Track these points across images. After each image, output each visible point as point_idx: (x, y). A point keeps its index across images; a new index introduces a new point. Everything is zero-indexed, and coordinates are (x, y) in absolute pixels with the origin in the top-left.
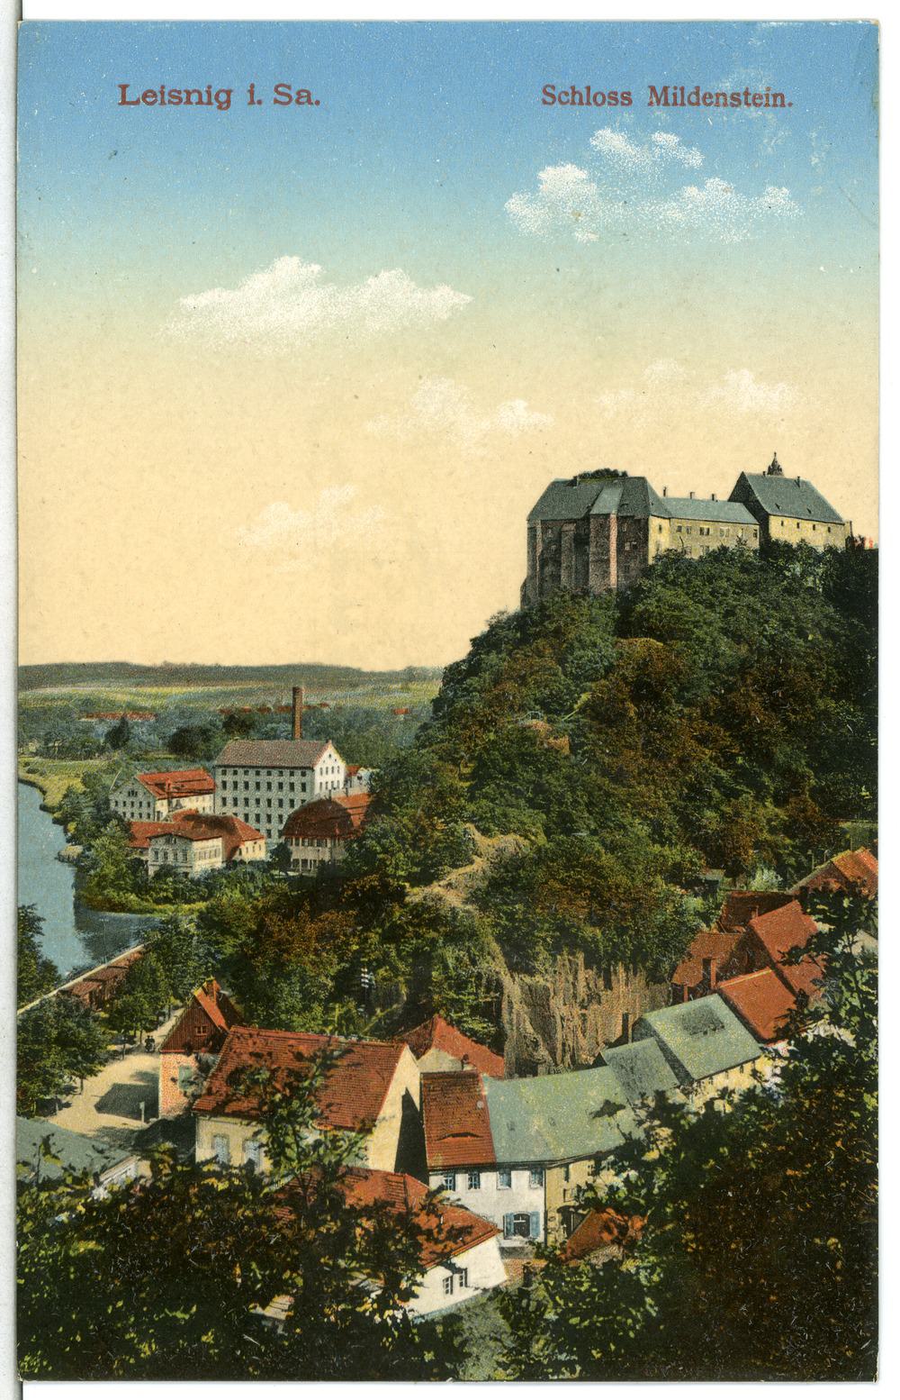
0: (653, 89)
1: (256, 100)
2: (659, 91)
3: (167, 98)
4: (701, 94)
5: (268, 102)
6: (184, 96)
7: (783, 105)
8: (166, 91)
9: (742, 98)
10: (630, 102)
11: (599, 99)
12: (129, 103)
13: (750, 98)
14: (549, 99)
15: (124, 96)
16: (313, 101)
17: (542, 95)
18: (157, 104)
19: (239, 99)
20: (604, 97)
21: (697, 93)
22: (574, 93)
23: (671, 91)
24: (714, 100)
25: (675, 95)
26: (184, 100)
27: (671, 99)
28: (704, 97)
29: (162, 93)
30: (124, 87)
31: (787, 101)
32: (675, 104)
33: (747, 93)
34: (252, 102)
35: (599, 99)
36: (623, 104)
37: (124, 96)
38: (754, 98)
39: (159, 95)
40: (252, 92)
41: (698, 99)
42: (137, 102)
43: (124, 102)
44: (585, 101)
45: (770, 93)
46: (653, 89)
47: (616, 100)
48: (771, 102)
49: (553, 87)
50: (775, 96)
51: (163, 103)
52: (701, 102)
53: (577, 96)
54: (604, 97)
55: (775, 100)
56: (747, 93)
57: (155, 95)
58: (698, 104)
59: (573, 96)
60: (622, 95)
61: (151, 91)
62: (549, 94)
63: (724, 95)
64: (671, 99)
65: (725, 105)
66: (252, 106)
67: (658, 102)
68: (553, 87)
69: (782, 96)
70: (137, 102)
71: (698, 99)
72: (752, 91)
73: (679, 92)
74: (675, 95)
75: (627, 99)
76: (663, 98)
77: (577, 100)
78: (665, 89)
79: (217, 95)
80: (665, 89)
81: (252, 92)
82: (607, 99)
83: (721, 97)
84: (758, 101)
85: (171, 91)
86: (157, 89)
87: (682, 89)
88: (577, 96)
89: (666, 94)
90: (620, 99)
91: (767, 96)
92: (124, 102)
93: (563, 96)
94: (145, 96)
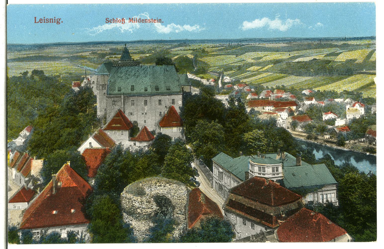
0: (130, 19)
2: (131, 19)
3: (46, 21)
4: (141, 20)
13: (153, 22)
15: (35, 20)
21: (140, 20)
24: (144, 21)
26: (49, 22)
29: (44, 19)
30: (35, 18)
31: (162, 21)
37: (35, 20)
39: (43, 20)
42: (38, 22)
43: (35, 22)
45: (158, 19)
48: (158, 21)
50: (159, 20)
51: (44, 22)
57: (42, 20)
58: (140, 22)
60: (48, 21)
61: (41, 19)
66: (45, 23)
67: (131, 22)
69: (161, 20)
70: (38, 22)
74: (135, 20)
78: (132, 18)
84: (155, 21)
86: (43, 19)
87: (136, 19)
94: (40, 20)
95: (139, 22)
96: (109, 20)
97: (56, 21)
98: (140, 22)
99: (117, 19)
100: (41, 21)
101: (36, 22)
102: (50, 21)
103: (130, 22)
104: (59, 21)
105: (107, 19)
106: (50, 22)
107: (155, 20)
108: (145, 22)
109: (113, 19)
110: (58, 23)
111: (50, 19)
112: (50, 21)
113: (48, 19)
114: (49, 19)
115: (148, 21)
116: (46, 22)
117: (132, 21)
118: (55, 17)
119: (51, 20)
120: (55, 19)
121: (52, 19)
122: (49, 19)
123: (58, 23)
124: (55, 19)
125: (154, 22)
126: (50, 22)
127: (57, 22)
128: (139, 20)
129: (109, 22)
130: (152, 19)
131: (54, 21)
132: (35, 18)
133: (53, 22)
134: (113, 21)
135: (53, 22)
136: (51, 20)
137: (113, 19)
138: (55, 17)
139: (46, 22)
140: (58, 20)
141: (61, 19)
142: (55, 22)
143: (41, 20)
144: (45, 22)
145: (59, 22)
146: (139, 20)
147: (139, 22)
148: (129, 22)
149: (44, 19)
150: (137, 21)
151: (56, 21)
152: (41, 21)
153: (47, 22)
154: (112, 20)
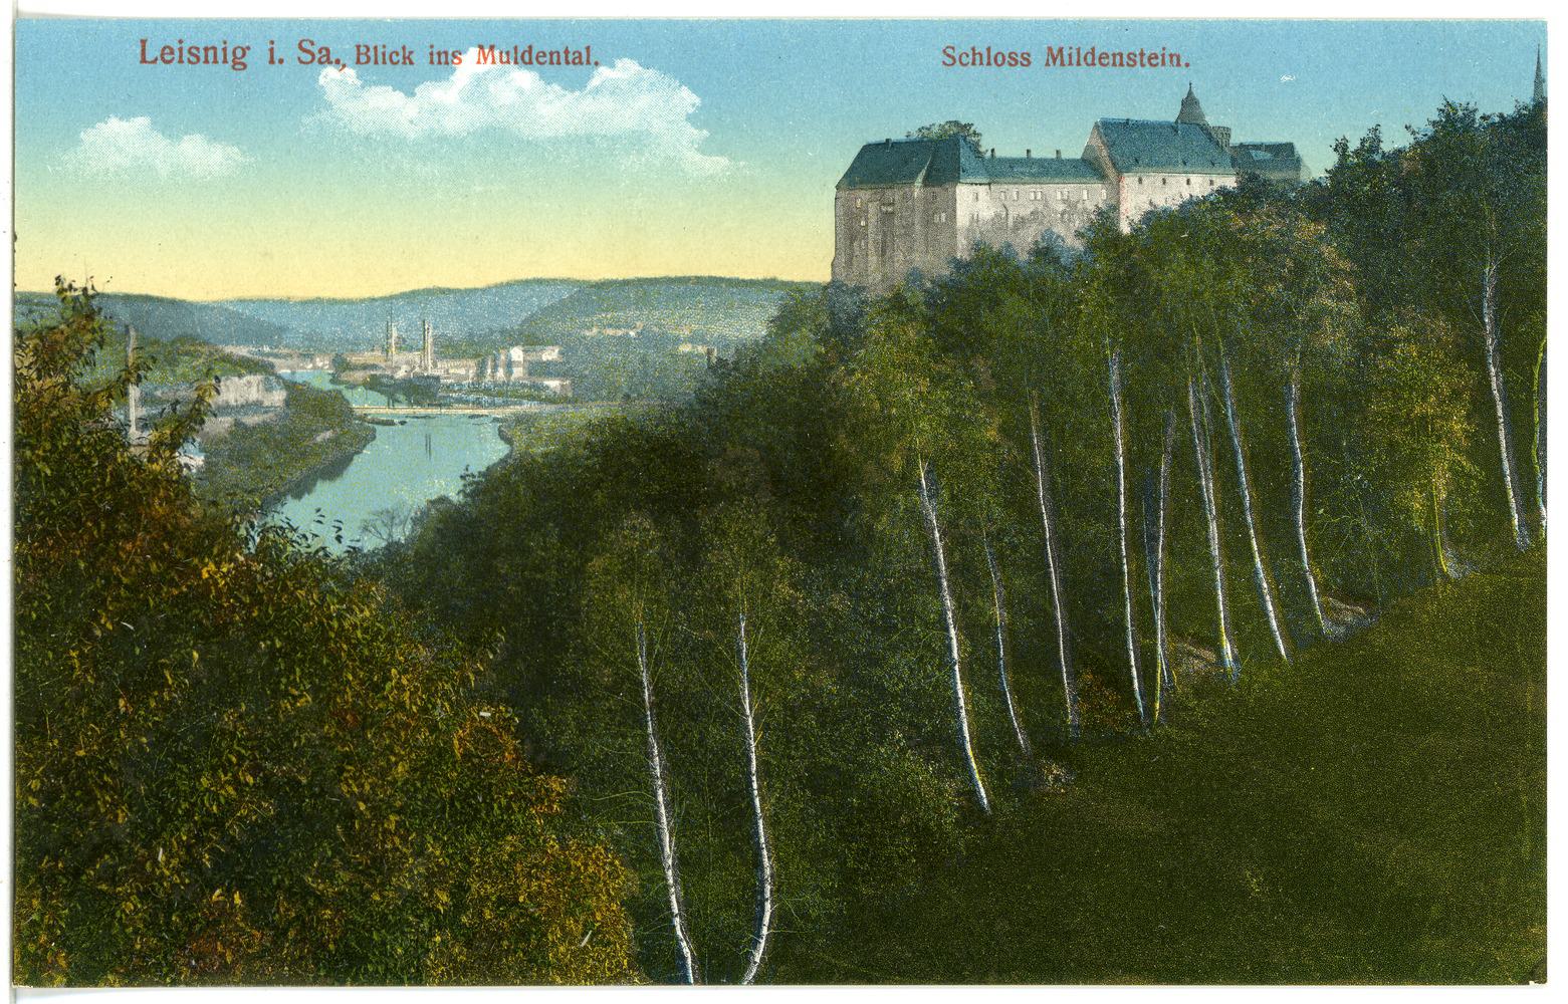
0: (1050, 49)
1: (277, 57)
2: (1055, 52)
4: (1097, 55)
5: (291, 62)
6: (202, 54)
7: (1178, 65)
8: (186, 46)
9: (1138, 59)
10: (1029, 63)
11: (1000, 58)
12: (149, 63)
13: (1145, 61)
14: (949, 61)
16: (333, 59)
18: (175, 62)
20: (1004, 59)
22: (974, 54)
23: (1066, 53)
25: (1070, 55)
26: (202, 59)
27: (1066, 61)
28: (1100, 58)
29: (181, 49)
30: (143, 42)
31: (1182, 63)
32: (1070, 64)
33: (1142, 54)
34: (272, 62)
35: (1000, 61)
36: (1022, 65)
38: (1150, 59)
39: (177, 54)
40: (272, 50)
41: (1093, 59)
42: (156, 59)
43: (144, 61)
46: (1050, 49)
47: (1016, 62)
51: (181, 61)
52: (1096, 61)
54: (1004, 59)
56: (1142, 54)
57: (172, 53)
58: (1094, 64)
61: (168, 47)
62: (949, 56)
64: (1066, 61)
65: (1121, 64)
67: (1054, 63)
71: (1093, 59)
74: (1070, 55)
76: (1058, 62)
77: (978, 62)
78: (1061, 50)
79: (234, 53)
80: (1061, 50)
81: (272, 50)
82: (1008, 59)
83: (1118, 58)
84: (1154, 62)
85: (190, 49)
86: (176, 46)
87: (1078, 50)
89: (1062, 57)
90: (1019, 59)
91: (1163, 55)
92: (144, 61)
94: (162, 55)
95: (1089, 60)
97: (230, 57)
99: (989, 49)
100: (166, 55)
101: (149, 58)
102: (206, 56)
104: (244, 55)
105: (950, 51)
106: (206, 62)
107: (1157, 57)
108: (1114, 64)
109: (973, 49)
110: (239, 64)
111: (206, 49)
112: (206, 56)
113: (198, 49)
114: (201, 46)
115: (1125, 59)
116: (189, 61)
117: (1058, 62)
118: (225, 43)
119: (211, 53)
120: (225, 50)
121: (214, 48)
122: (201, 46)
123: (237, 67)
124: (225, 50)
125: (1151, 65)
126: (206, 62)
127: (233, 61)
128: (1089, 58)
129: (958, 63)
132: (143, 42)
133: (215, 62)
135: (215, 62)
136: (211, 53)
137: (973, 49)
139: (189, 61)
140: (239, 53)
141: (248, 48)
142: (225, 61)
143: (167, 51)
144: (185, 59)
145: (243, 60)
146: (1089, 58)
147: (1089, 60)
148: (1047, 64)
149: (181, 49)
150: (1082, 59)
151: (230, 57)
153: (194, 59)
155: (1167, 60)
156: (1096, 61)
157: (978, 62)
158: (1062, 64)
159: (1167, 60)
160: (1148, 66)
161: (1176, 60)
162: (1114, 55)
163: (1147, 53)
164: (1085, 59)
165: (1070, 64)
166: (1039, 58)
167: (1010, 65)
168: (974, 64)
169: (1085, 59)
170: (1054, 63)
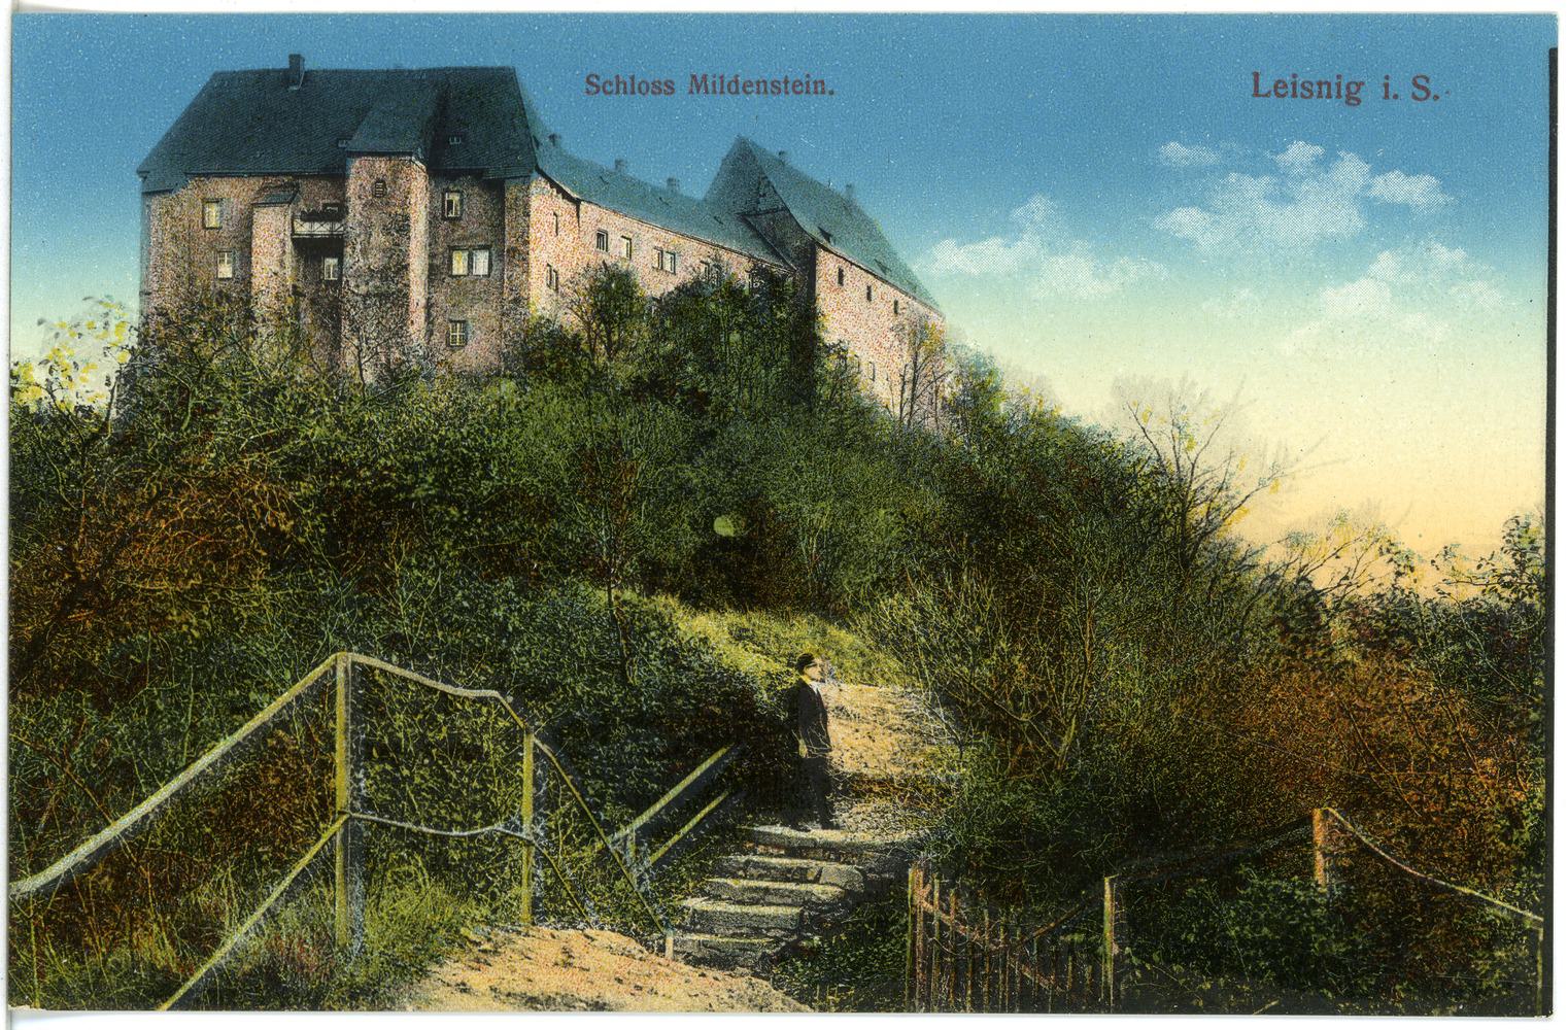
2: (699, 80)
4: (740, 87)
7: (823, 92)
9: (782, 86)
11: (644, 87)
13: (790, 86)
17: (584, 86)
19: (1371, 94)
23: (709, 83)
24: (755, 88)
25: (714, 83)
27: (710, 87)
28: (744, 86)
35: (644, 87)
38: (794, 86)
44: (718, 90)
46: (694, 77)
49: (597, 77)
50: (815, 83)
52: (740, 90)
53: (622, 86)
55: (816, 88)
58: (737, 92)
59: (618, 86)
63: (765, 82)
64: (710, 87)
67: (698, 90)
68: (597, 77)
69: (822, 82)
72: (791, 79)
73: (718, 81)
74: (714, 83)
75: (670, 88)
76: (702, 90)
78: (705, 77)
80: (705, 77)
83: (762, 85)
87: (722, 77)
88: (622, 86)
91: (808, 83)
93: (608, 88)
95: (733, 89)
96: (601, 85)
98: (737, 92)
99: (632, 78)
103: (695, 91)
109: (617, 77)
115: (769, 85)
117: (702, 90)
129: (601, 93)
130: (786, 82)
131: (1334, 93)
134: (618, 86)
137: (617, 77)
138: (808, 76)
147: (733, 89)
148: (691, 92)
150: (725, 84)
152: (1281, 91)
154: (611, 84)
155: (812, 87)
156: (740, 90)
157: (762, 90)
158: (707, 92)
159: (812, 87)
160: (791, 93)
161: (819, 87)
162: (758, 83)
163: (791, 79)
164: (729, 85)
165: (714, 92)
166: (682, 85)
167: (653, 93)
168: (618, 92)
169: (729, 90)
170: (698, 90)
